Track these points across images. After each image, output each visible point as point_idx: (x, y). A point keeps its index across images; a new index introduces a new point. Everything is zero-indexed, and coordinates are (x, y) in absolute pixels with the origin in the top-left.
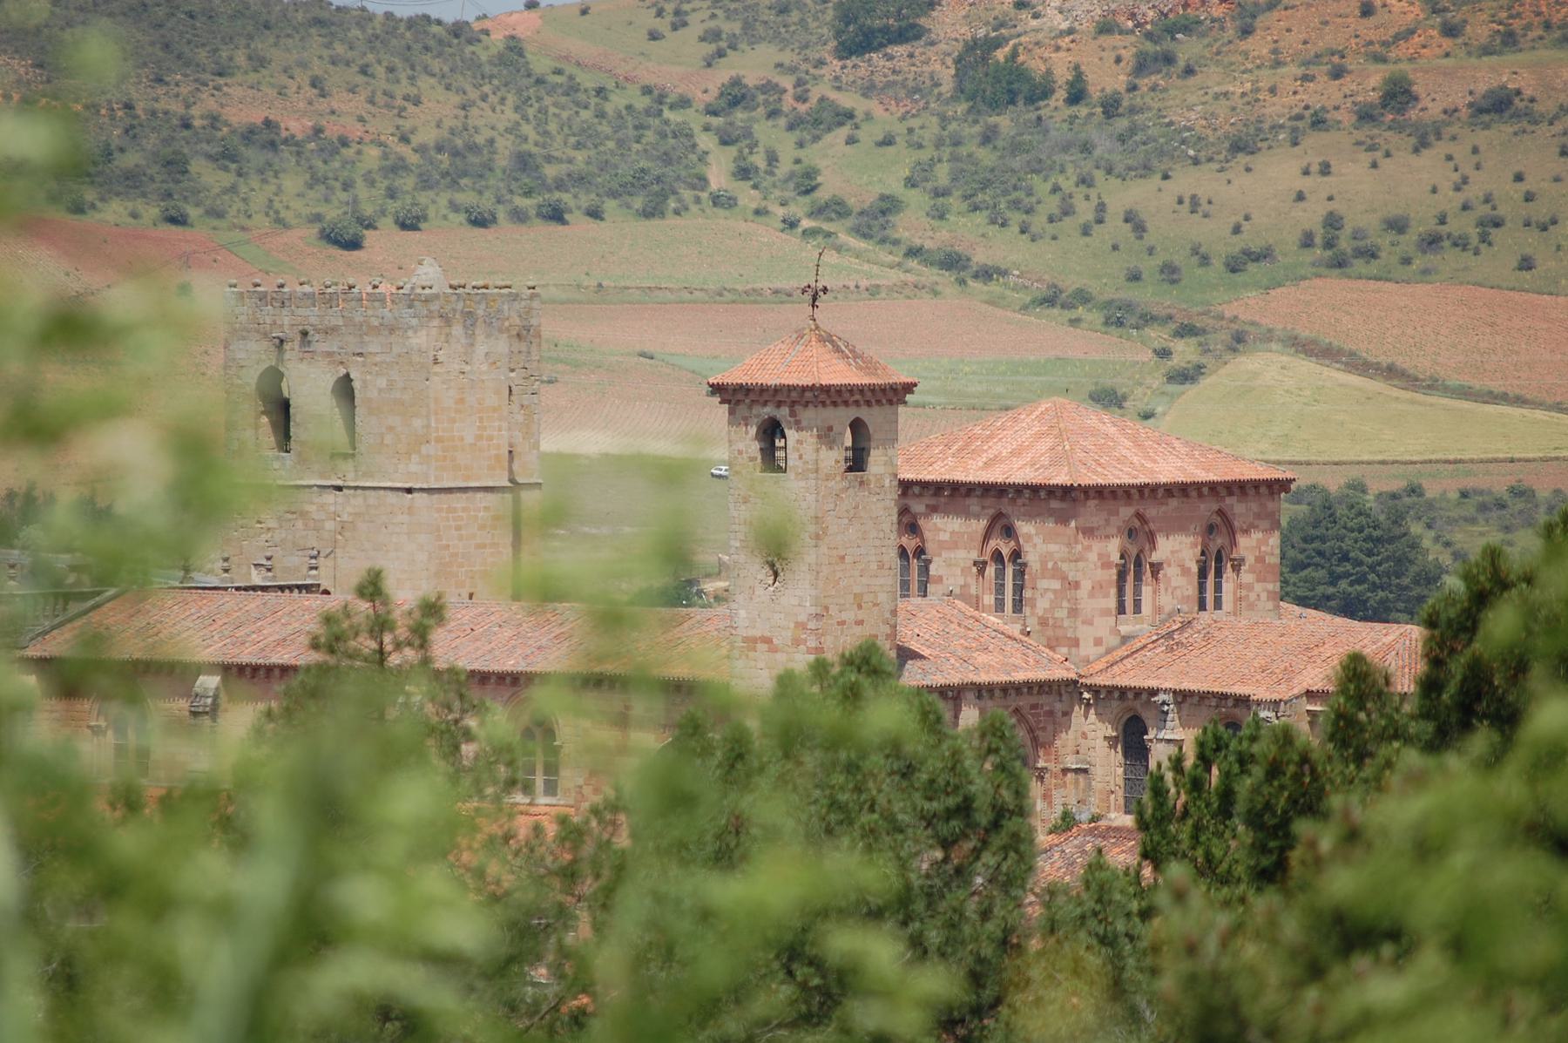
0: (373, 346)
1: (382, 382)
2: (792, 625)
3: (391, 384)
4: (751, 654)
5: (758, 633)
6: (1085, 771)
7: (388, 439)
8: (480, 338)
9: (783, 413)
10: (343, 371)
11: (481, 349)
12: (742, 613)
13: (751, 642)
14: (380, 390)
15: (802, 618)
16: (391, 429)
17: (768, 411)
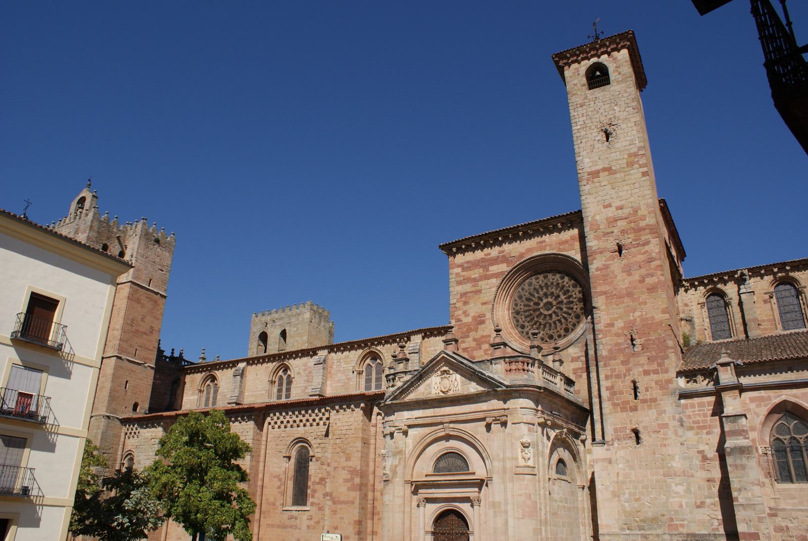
0: (293, 320)
1: (295, 329)
2: (626, 156)
3: (298, 328)
4: (595, 180)
5: (599, 167)
6: (690, 321)
7: (295, 344)
8: (322, 321)
9: (604, 59)
10: (283, 329)
11: (322, 324)
12: (586, 160)
13: (595, 174)
14: (294, 331)
15: (634, 150)
16: (296, 341)
17: (594, 60)
